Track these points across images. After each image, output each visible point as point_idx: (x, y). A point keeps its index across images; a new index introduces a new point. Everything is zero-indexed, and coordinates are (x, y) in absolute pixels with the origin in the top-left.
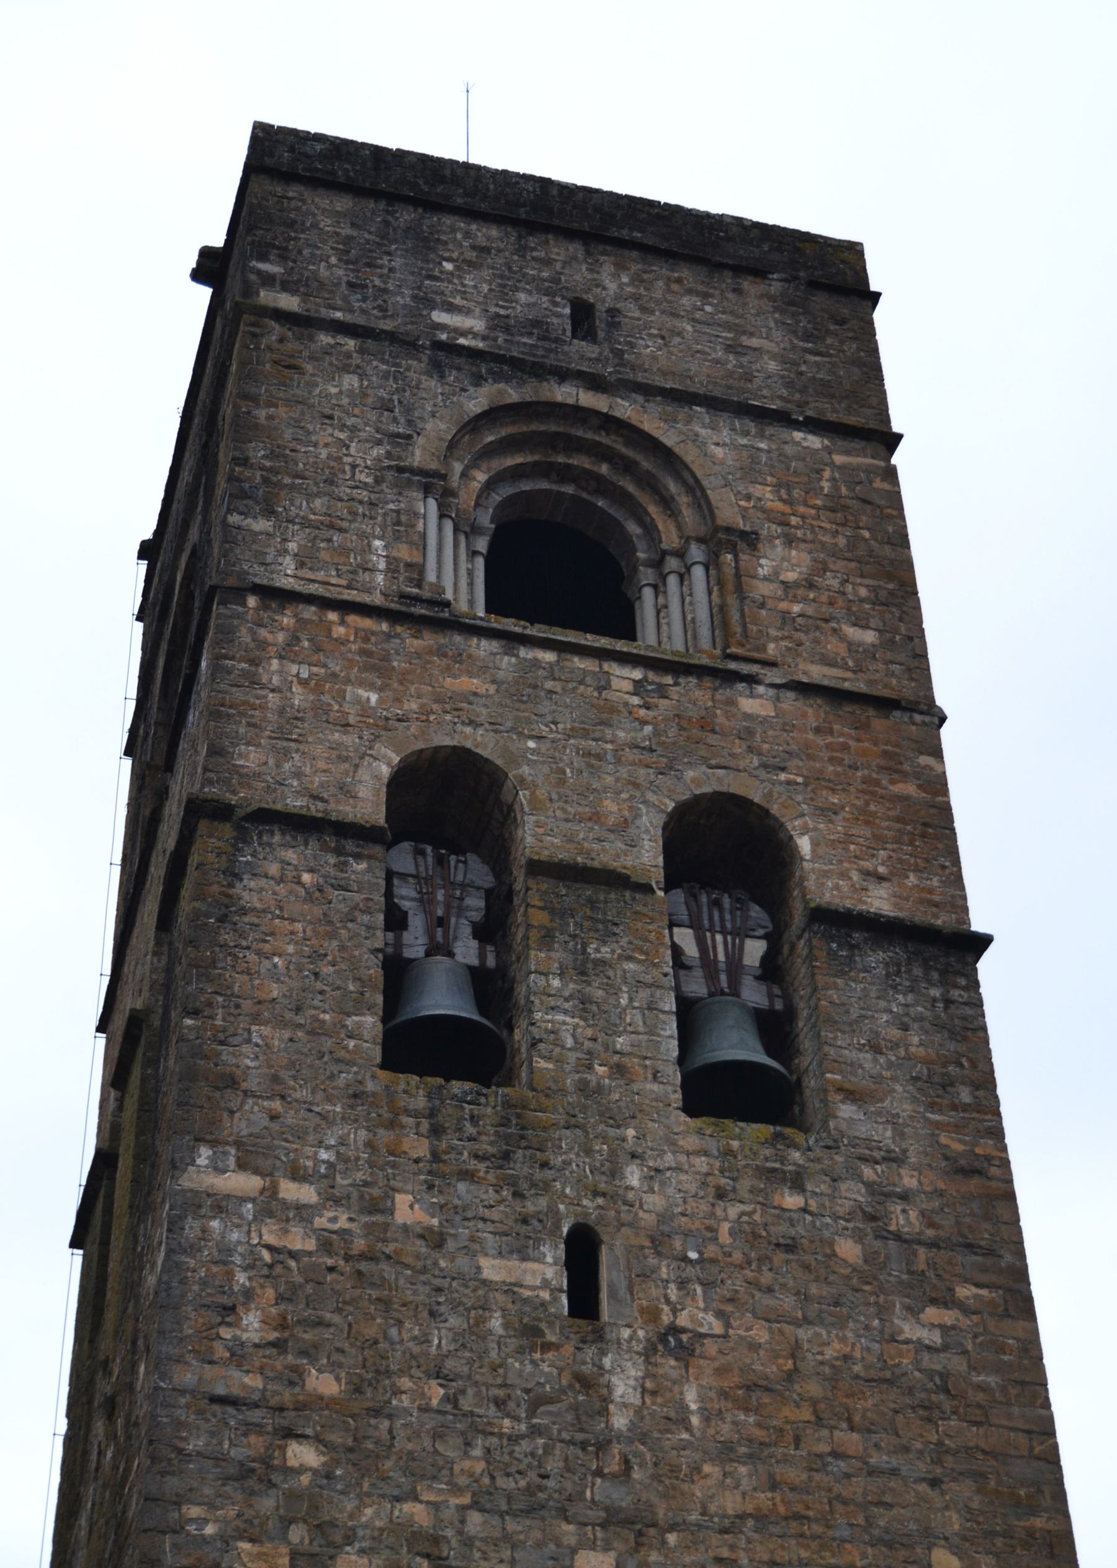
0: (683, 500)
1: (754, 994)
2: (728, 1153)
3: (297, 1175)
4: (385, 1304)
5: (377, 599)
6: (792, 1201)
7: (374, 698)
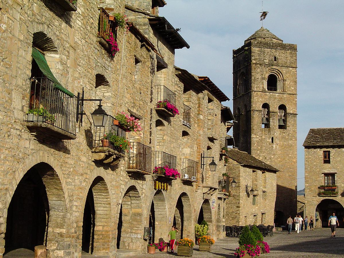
0: (281, 75)
1: (283, 118)
2: (281, 131)
3: (258, 135)
4: (262, 143)
5: (261, 91)
6: (284, 134)
7: (261, 99)
